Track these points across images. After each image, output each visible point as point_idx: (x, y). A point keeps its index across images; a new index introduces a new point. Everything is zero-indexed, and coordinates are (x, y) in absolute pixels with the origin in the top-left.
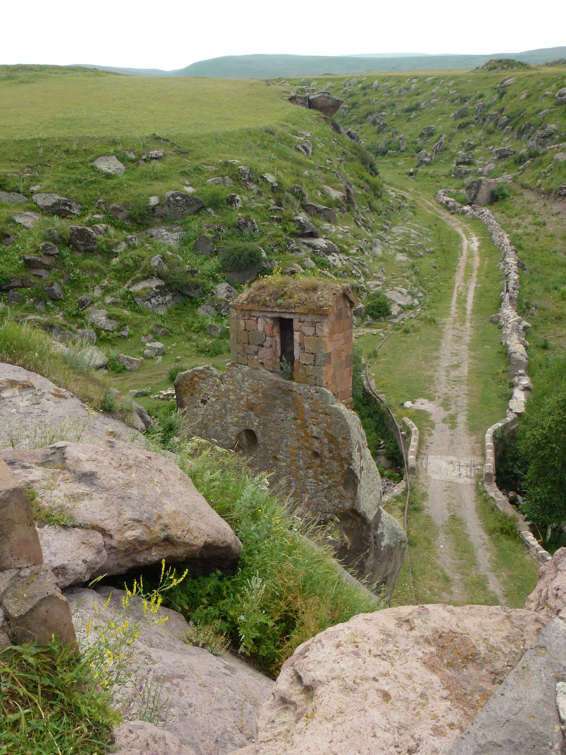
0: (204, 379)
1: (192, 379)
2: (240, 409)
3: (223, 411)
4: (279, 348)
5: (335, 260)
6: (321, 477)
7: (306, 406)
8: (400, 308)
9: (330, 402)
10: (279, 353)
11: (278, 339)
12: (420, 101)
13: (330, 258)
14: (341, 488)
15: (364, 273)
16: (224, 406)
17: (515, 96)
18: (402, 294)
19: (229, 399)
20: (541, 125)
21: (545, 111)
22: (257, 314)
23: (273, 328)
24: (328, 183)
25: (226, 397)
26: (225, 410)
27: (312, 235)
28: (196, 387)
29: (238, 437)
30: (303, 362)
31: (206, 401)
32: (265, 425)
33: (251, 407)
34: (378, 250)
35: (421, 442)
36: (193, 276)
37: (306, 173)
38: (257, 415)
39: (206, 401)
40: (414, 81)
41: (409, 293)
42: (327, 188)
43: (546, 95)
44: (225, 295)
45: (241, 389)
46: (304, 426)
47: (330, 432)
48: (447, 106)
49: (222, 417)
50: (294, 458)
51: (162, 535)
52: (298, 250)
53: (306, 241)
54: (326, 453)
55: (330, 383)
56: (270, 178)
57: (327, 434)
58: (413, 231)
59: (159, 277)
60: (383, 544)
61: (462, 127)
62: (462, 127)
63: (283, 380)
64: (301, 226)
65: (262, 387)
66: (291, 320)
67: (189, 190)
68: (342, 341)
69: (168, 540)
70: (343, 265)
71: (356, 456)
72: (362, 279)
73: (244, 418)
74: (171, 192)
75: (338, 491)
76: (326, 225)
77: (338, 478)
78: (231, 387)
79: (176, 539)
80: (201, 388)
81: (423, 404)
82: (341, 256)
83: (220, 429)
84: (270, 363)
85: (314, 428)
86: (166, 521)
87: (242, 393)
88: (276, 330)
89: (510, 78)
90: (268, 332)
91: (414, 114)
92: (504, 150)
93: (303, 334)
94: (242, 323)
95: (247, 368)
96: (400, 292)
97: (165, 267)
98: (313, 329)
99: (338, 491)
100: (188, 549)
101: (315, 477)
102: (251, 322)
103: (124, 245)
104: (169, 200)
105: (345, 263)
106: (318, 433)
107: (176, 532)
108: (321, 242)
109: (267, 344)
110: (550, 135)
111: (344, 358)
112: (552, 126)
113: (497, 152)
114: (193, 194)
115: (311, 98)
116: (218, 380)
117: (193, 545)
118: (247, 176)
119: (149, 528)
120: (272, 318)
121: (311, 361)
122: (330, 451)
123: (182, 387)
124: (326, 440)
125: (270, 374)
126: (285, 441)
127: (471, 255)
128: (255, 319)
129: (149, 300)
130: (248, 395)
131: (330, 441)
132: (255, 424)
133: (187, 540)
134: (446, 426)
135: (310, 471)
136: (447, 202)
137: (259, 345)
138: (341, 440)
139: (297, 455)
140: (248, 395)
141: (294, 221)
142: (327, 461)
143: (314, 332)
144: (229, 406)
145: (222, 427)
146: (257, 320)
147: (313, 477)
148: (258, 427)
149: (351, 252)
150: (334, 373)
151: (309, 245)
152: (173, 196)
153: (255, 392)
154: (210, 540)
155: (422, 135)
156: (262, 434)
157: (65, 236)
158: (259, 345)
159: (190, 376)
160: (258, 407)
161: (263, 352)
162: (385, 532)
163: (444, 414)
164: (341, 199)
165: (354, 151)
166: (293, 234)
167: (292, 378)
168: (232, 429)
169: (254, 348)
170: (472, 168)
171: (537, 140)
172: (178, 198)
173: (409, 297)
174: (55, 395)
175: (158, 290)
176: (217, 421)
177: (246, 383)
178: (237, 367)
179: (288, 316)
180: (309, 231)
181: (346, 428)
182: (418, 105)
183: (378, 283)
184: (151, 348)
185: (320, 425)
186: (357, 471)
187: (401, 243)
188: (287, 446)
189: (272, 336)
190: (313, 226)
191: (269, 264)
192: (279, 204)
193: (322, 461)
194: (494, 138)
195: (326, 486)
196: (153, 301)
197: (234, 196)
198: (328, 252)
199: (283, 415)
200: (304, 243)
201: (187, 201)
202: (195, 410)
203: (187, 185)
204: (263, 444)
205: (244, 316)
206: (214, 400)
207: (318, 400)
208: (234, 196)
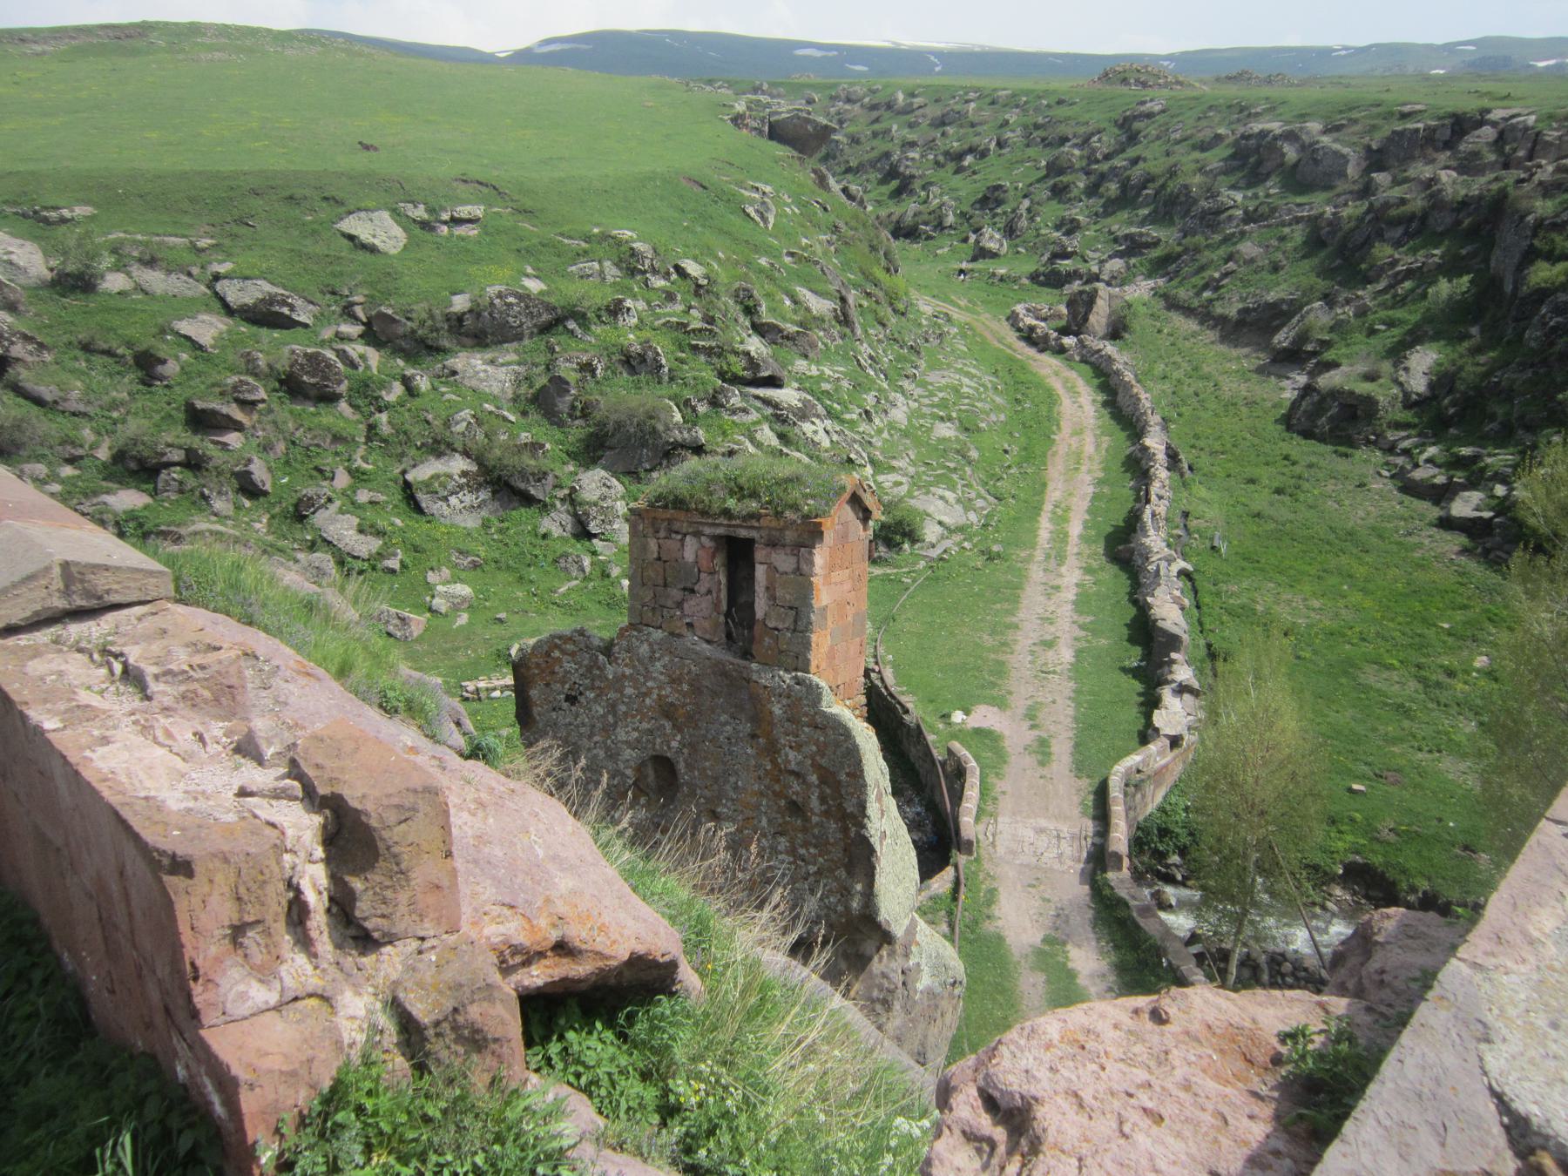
0: (573, 654)
1: (548, 654)
2: (644, 716)
3: (611, 719)
4: (724, 595)
5: (815, 432)
6: (802, 851)
7: (777, 710)
8: (939, 529)
9: (824, 704)
10: (724, 607)
11: (723, 579)
13: (807, 427)
14: (842, 873)
15: (872, 462)
16: (612, 708)
19: (623, 695)
23: (713, 556)
24: (807, 283)
27: (774, 382)
28: (557, 668)
29: (640, 769)
30: (771, 625)
31: (575, 698)
32: (693, 747)
33: (667, 711)
34: (899, 415)
35: (984, 792)
36: (534, 456)
37: (763, 261)
38: (678, 728)
39: (575, 698)
41: (959, 501)
42: (804, 293)
44: (598, 493)
45: (648, 677)
46: (772, 749)
47: (823, 762)
49: (608, 730)
50: (749, 813)
51: (554, 936)
52: (745, 411)
53: (761, 392)
54: (814, 803)
55: (823, 665)
56: (693, 268)
57: (817, 767)
58: (966, 381)
59: (466, 454)
60: (920, 986)
63: (731, 659)
64: (753, 364)
65: (689, 672)
66: (750, 543)
67: (534, 286)
68: (847, 586)
69: (562, 948)
71: (872, 809)
72: (869, 470)
73: (650, 732)
74: (497, 288)
75: (836, 879)
76: (801, 365)
77: (837, 853)
78: (628, 671)
79: (577, 944)
80: (567, 672)
81: (984, 717)
82: (828, 422)
83: (602, 754)
84: (706, 624)
85: (792, 755)
86: (561, 908)
87: (649, 684)
88: (719, 561)
90: (704, 563)
93: (772, 569)
94: (653, 545)
95: (658, 635)
96: (942, 498)
97: (480, 437)
98: (793, 560)
99: (836, 879)
100: (600, 964)
101: (792, 851)
102: (672, 544)
103: (398, 389)
104: (492, 304)
105: (835, 437)
106: (798, 764)
107: (577, 933)
108: (788, 396)
109: (702, 588)
111: (850, 619)
114: (542, 293)
116: (601, 657)
117: (608, 958)
118: (647, 262)
119: (529, 921)
120: (714, 538)
121: (789, 623)
123: (529, 668)
124: (814, 778)
125: (705, 646)
126: (733, 779)
127: (1078, 432)
129: (445, 499)
130: (660, 688)
131: (823, 781)
132: (674, 744)
133: (599, 948)
134: (1030, 761)
135: (782, 839)
136: (1032, 329)
137: (685, 589)
138: (843, 777)
139: (757, 807)
140: (660, 688)
141: (736, 353)
142: (815, 819)
145: (608, 749)
146: (682, 541)
147: (787, 853)
148: (679, 751)
149: (847, 416)
150: (832, 648)
151: (767, 402)
152: (500, 295)
153: (675, 681)
154: (641, 949)
156: (688, 765)
157: (278, 366)
158: (685, 589)
159: (546, 648)
160: (681, 711)
161: (692, 603)
162: (923, 961)
163: (1030, 736)
164: (829, 316)
165: (853, 223)
166: (736, 380)
167: (747, 654)
168: (628, 753)
169: (676, 594)
172: (511, 300)
173: (959, 508)
174: (299, 672)
175: (464, 480)
176: (596, 738)
177: (658, 664)
178: (640, 631)
180: (766, 374)
181: (853, 755)
183: (899, 478)
184: (446, 595)
185: (805, 749)
186: (875, 841)
187: (943, 404)
188: (736, 788)
189: (712, 573)
190: (775, 365)
192: (710, 320)
193: (806, 820)
195: (812, 869)
196: (453, 500)
197: (620, 301)
199: (728, 728)
200: (757, 397)
201: (527, 307)
202: (554, 715)
203: (527, 276)
204: (687, 783)
208: (620, 301)
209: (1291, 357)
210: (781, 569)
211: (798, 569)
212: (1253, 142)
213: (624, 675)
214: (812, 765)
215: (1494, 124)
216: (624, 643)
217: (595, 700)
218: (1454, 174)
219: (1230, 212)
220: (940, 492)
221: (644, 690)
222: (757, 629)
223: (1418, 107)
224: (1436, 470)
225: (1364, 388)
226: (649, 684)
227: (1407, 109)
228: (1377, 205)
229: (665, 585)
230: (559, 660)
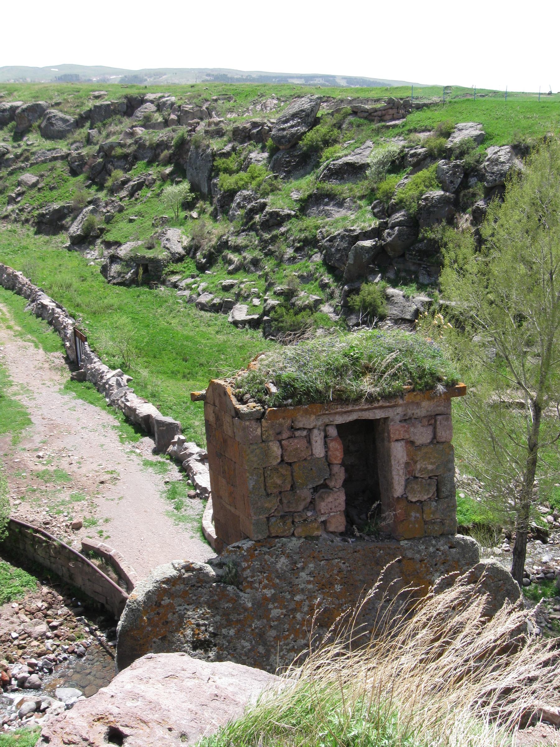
1: (158, 604)
3: (261, 649)
19: (269, 620)
25: (260, 618)
26: (265, 644)
65: (340, 571)
78: (269, 593)
87: (298, 598)
94: (276, 450)
95: (294, 543)
116: (230, 588)
128: (305, 433)
140: (311, 597)
143: (431, 437)
144: (273, 633)
161: (330, 499)
177: (303, 574)
179: (379, 415)
205: (279, 433)
206: (232, 632)
207: (459, 561)
209: (82, 242)
210: (418, 442)
211: (435, 437)
212: (7, 113)
213: (265, 598)
215: (152, 102)
216: (257, 564)
217: (239, 635)
218: (143, 129)
219: (8, 156)
221: (292, 606)
223: (102, 93)
224: (212, 296)
225: (150, 254)
226: (298, 598)
227: (97, 93)
229: (293, 487)
230: (170, 606)
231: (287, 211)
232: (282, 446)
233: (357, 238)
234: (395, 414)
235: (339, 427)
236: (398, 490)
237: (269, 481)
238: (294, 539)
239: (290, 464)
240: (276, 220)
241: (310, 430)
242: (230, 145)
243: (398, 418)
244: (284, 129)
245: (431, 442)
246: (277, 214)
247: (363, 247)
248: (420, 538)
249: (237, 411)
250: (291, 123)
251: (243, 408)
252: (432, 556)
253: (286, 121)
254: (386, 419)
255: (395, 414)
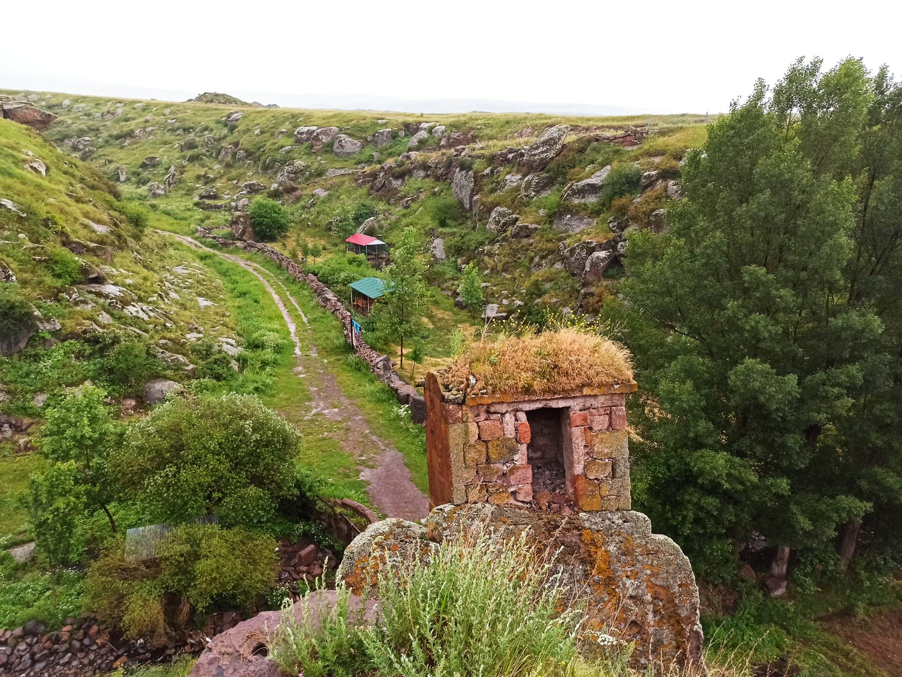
5: (137, 312)
7: (612, 548)
12: (132, 127)
17: (248, 130)
18: (232, 345)
20: (286, 160)
21: (287, 148)
22: (503, 408)
27: (99, 280)
40: (119, 105)
43: (282, 133)
48: (168, 136)
52: (84, 302)
61: (192, 159)
62: (192, 159)
70: (150, 317)
76: (107, 269)
85: (628, 582)
89: (237, 112)
91: (127, 142)
92: (254, 184)
94: (473, 428)
105: (152, 314)
108: (110, 289)
110: (298, 173)
112: (299, 163)
113: (246, 186)
115: (6, 107)
122: (655, 612)
124: (648, 597)
149: (150, 299)
151: (99, 294)
155: (144, 166)
170: (219, 203)
171: (288, 176)
179: (561, 404)
182: (132, 131)
191: (46, 324)
194: (234, 173)
198: (125, 303)
205: (478, 415)
211: (610, 425)
214: (647, 587)
215: (425, 129)
220: (225, 340)
222: (581, 484)
228: (386, 168)
231: (534, 226)
232: (479, 427)
233: (593, 250)
234: (575, 405)
235: (528, 413)
236: (578, 469)
237: (468, 456)
238: (487, 505)
239: (486, 442)
240: (526, 232)
241: (503, 415)
242: (490, 168)
243: (577, 408)
244: (535, 155)
245: (607, 429)
246: (527, 227)
247: (598, 258)
248: (597, 512)
249: (443, 397)
250: (541, 149)
251: (446, 394)
252: (610, 528)
253: (537, 148)
254: (568, 408)
255: (575, 405)
